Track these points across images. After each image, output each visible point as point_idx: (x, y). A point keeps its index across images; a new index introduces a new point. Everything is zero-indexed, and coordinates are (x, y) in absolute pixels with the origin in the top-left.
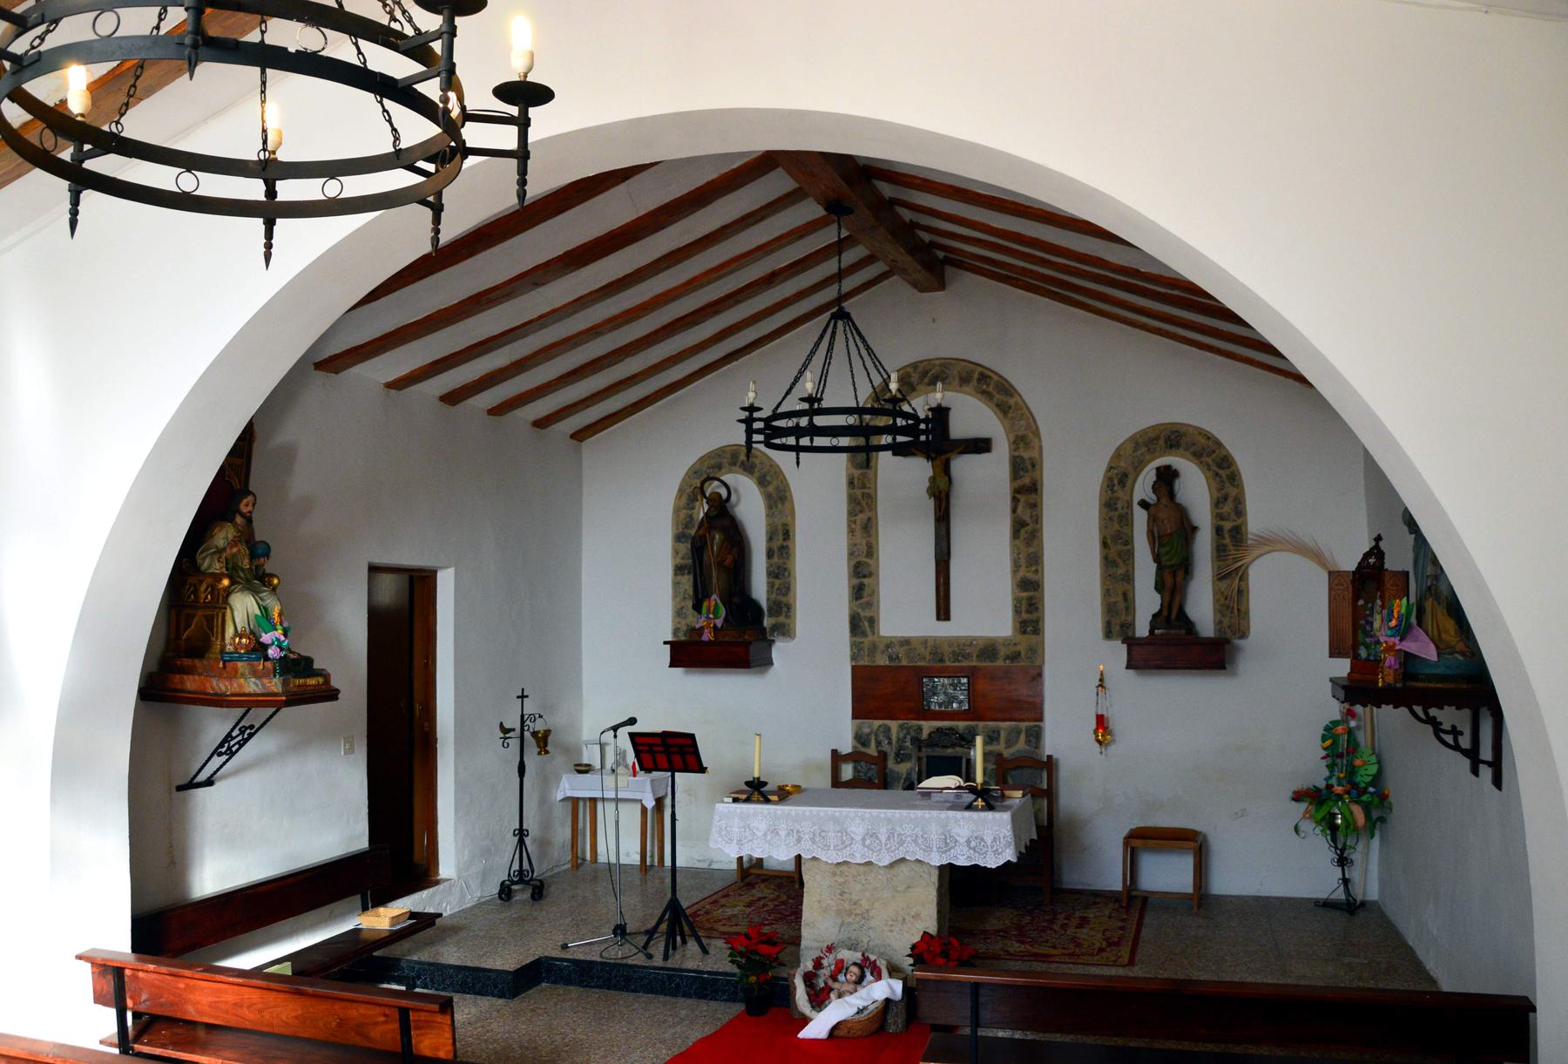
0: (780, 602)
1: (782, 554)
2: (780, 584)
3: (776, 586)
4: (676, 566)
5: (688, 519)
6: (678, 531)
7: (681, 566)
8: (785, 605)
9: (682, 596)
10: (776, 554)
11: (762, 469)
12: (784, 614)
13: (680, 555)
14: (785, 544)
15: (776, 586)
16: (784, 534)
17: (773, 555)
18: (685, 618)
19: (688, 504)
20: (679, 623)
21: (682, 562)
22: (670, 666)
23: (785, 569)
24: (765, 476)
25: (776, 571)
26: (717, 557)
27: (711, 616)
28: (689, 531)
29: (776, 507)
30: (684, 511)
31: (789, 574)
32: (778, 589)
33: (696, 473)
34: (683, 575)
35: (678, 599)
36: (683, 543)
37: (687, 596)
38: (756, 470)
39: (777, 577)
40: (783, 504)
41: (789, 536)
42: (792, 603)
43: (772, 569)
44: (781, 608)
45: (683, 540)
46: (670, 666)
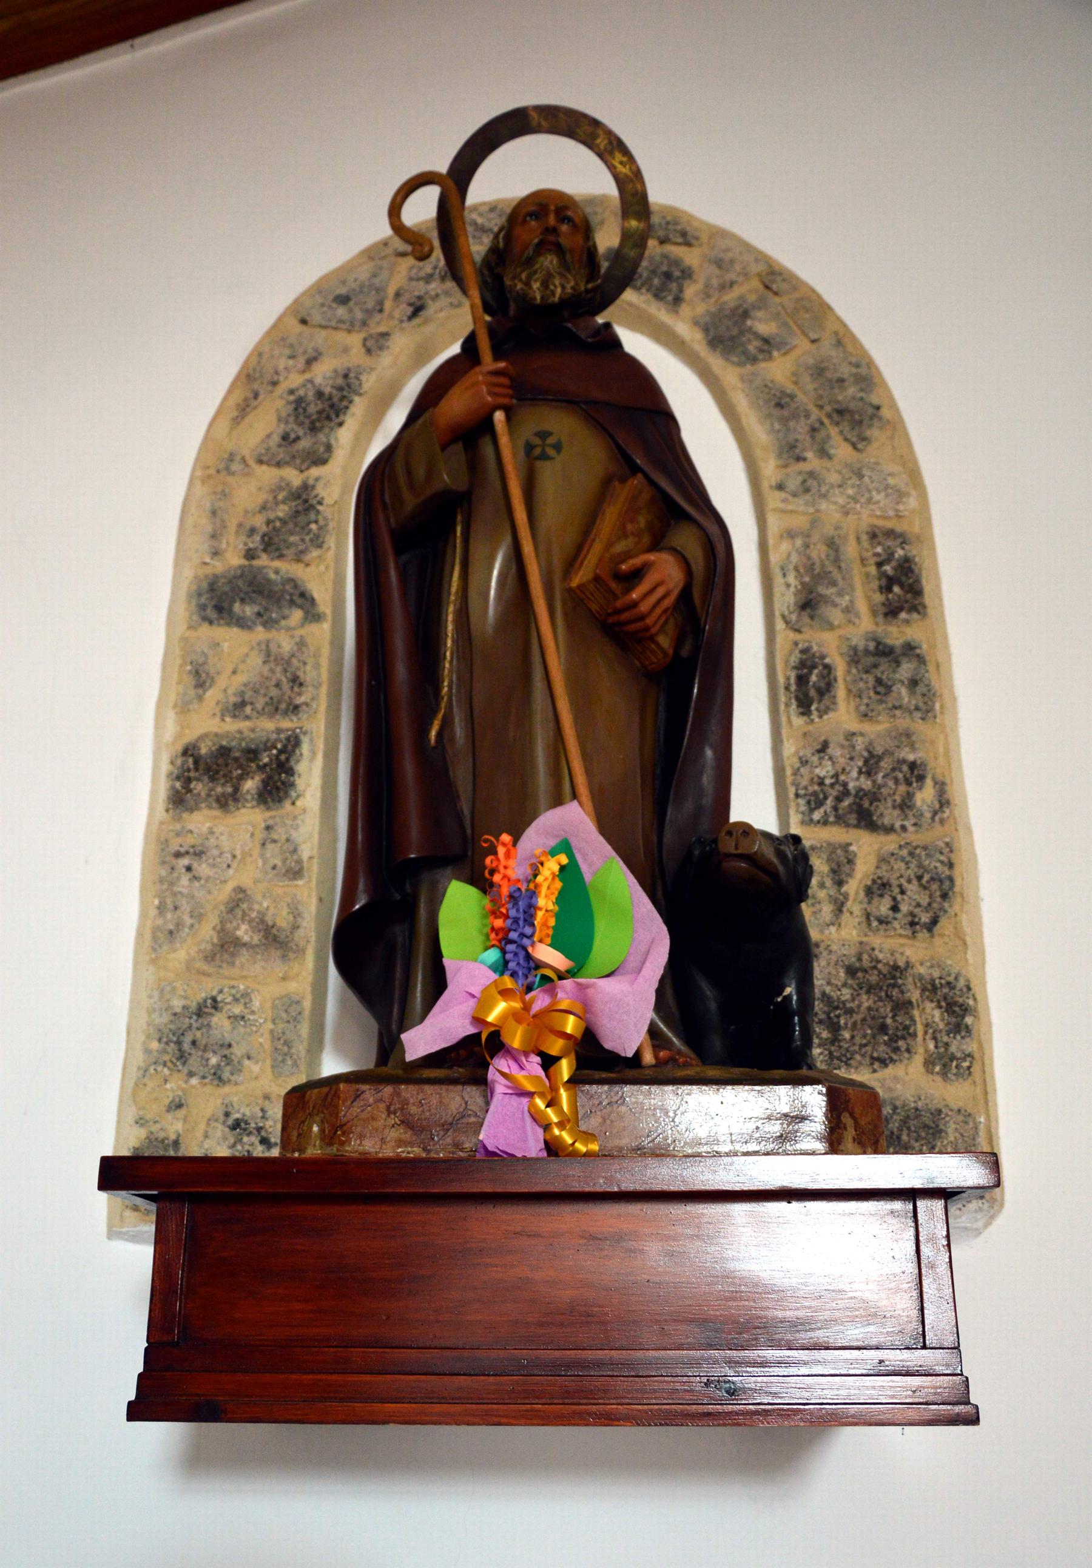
0: (896, 972)
1: (883, 687)
2: (883, 860)
3: (864, 869)
4: (188, 751)
5: (283, 511)
6: (218, 567)
7: (224, 752)
8: (931, 989)
9: (207, 932)
10: (840, 691)
11: (724, 287)
12: (924, 1045)
13: (212, 695)
14: (896, 634)
15: (864, 869)
16: (888, 584)
17: (826, 689)
18: (218, 1078)
19: (287, 439)
20: (177, 1105)
21: (231, 726)
22: (137, 1411)
23: (916, 773)
24: (742, 313)
25: (855, 781)
26: (571, 564)
27: (547, 954)
28: (287, 568)
29: (823, 453)
30: (268, 475)
31: (943, 802)
32: (877, 888)
33: (343, 300)
34: (224, 803)
35: (181, 954)
36: (242, 623)
37: (243, 932)
38: (690, 291)
39: (866, 820)
40: (858, 443)
41: (915, 590)
42: (971, 973)
43: (825, 770)
44: (903, 1006)
45: (249, 610)
46: (137, 1411)
